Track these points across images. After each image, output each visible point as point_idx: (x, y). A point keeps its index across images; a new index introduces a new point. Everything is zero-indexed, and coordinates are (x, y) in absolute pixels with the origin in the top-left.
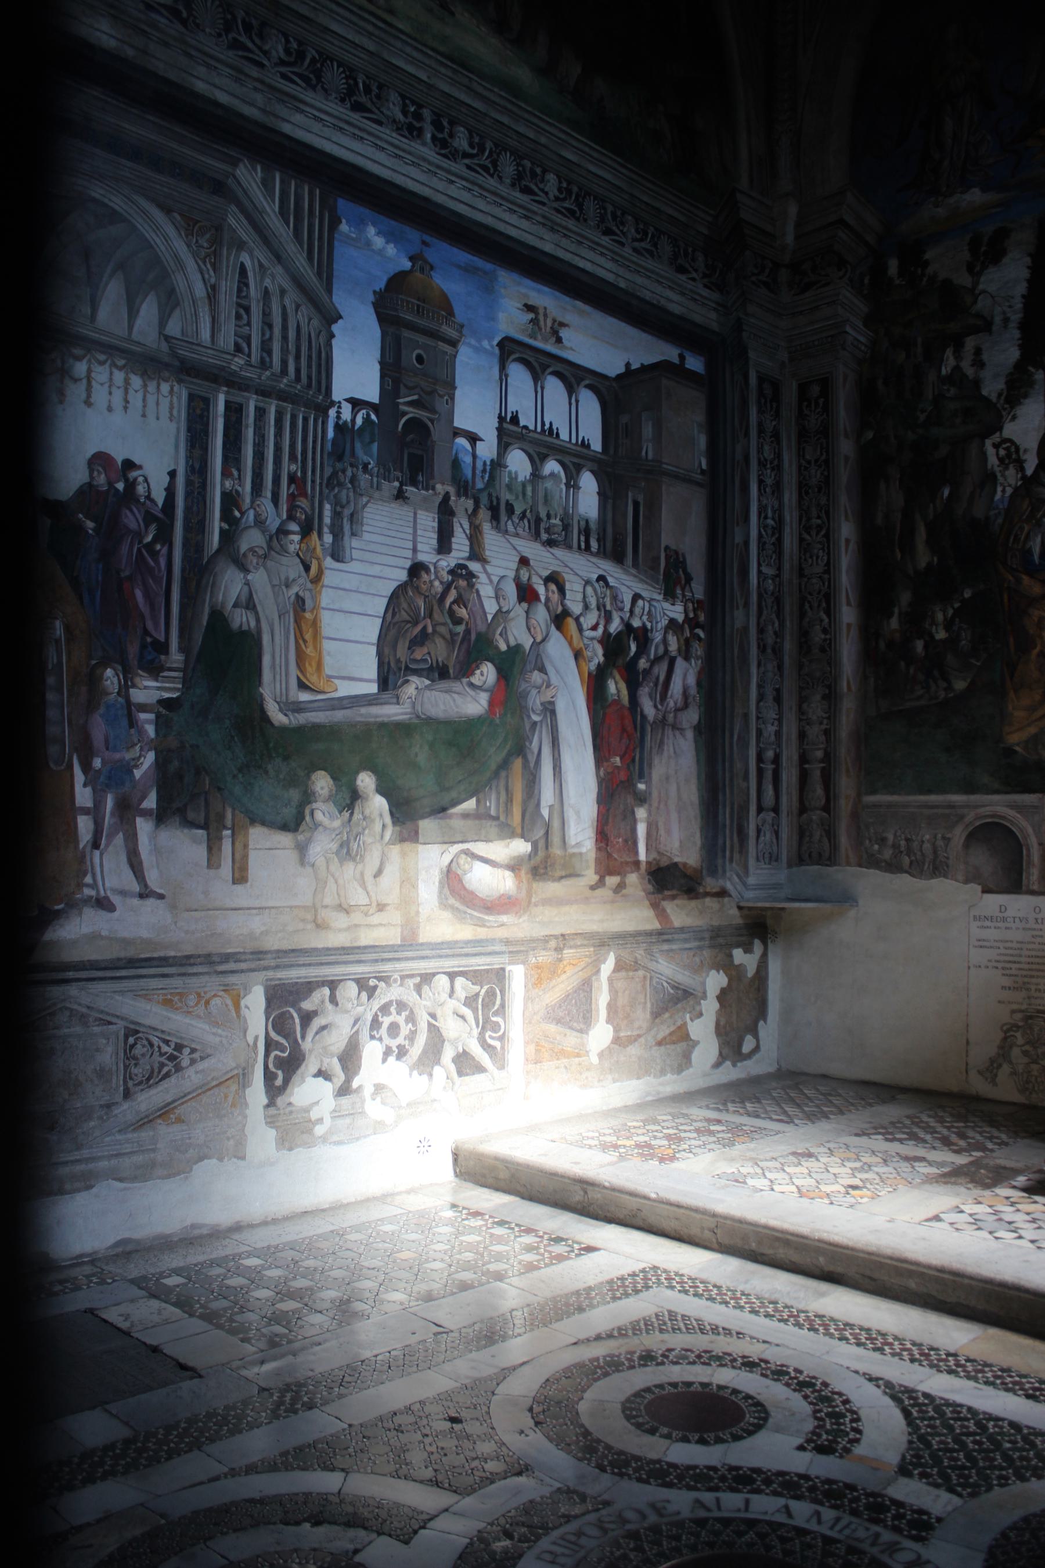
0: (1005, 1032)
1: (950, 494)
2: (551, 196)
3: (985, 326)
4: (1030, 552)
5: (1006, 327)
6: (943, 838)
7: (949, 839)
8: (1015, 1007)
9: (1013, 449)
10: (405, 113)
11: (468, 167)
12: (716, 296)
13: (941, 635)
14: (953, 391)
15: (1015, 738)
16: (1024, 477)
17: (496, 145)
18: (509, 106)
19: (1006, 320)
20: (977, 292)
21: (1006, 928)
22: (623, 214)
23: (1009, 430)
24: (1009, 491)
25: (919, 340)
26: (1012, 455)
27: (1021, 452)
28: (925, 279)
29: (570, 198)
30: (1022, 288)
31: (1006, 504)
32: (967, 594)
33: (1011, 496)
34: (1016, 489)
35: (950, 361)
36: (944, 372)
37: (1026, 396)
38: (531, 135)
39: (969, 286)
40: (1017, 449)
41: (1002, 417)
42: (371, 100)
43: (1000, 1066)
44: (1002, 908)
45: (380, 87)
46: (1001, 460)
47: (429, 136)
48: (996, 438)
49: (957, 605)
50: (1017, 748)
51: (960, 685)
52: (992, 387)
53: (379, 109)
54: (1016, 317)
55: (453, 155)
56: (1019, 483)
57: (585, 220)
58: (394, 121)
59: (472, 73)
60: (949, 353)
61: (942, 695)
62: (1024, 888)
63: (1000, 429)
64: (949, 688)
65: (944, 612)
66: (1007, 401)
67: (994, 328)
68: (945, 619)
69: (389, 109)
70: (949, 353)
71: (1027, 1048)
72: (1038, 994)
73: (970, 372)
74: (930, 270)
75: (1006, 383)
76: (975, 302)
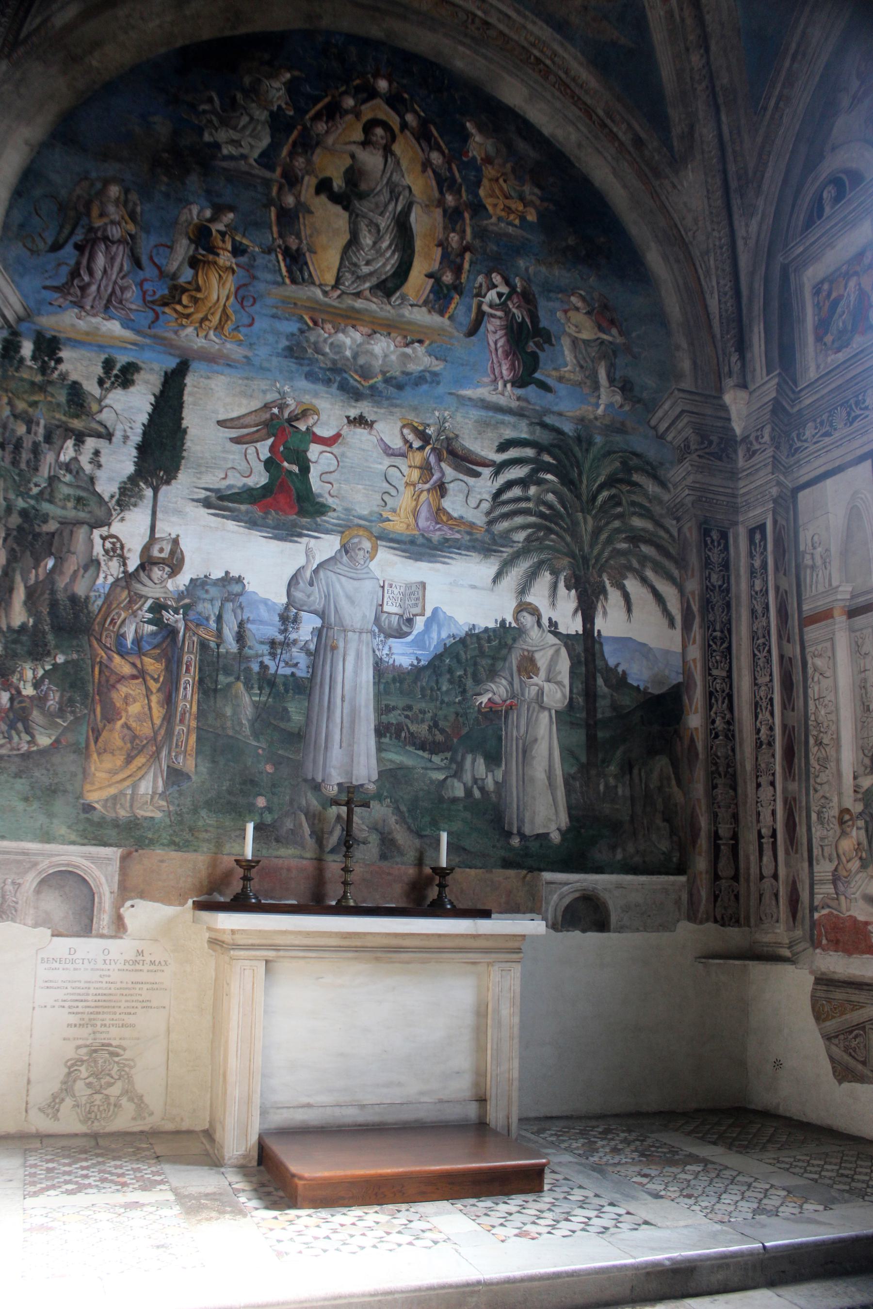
0: (69, 1068)
1: (54, 566)
3: (109, 436)
4: (123, 636)
5: (124, 442)
6: (13, 883)
7: (19, 884)
8: (80, 1042)
9: (118, 545)
13: (28, 691)
14: (68, 478)
15: (95, 796)
16: (125, 572)
19: (126, 438)
20: (103, 404)
21: (75, 969)
23: (116, 528)
24: (111, 580)
25: (42, 422)
26: (117, 550)
27: (125, 551)
28: (56, 373)
30: (144, 418)
31: (107, 590)
32: (60, 659)
33: (113, 584)
34: (117, 580)
35: (68, 452)
36: (62, 458)
37: (135, 505)
39: (98, 396)
40: (122, 547)
41: (111, 515)
43: (63, 1100)
44: (72, 951)
46: (107, 552)
48: (104, 531)
49: (48, 667)
50: (96, 805)
51: (44, 741)
52: (107, 487)
54: (136, 438)
56: (121, 575)
60: (70, 443)
61: (25, 747)
62: (94, 932)
63: (109, 525)
64: (33, 742)
65: (34, 670)
66: (119, 503)
67: (114, 439)
68: (35, 678)
70: (70, 443)
71: (91, 1079)
72: (103, 1029)
73: (88, 468)
74: (62, 367)
75: (120, 488)
76: (101, 411)
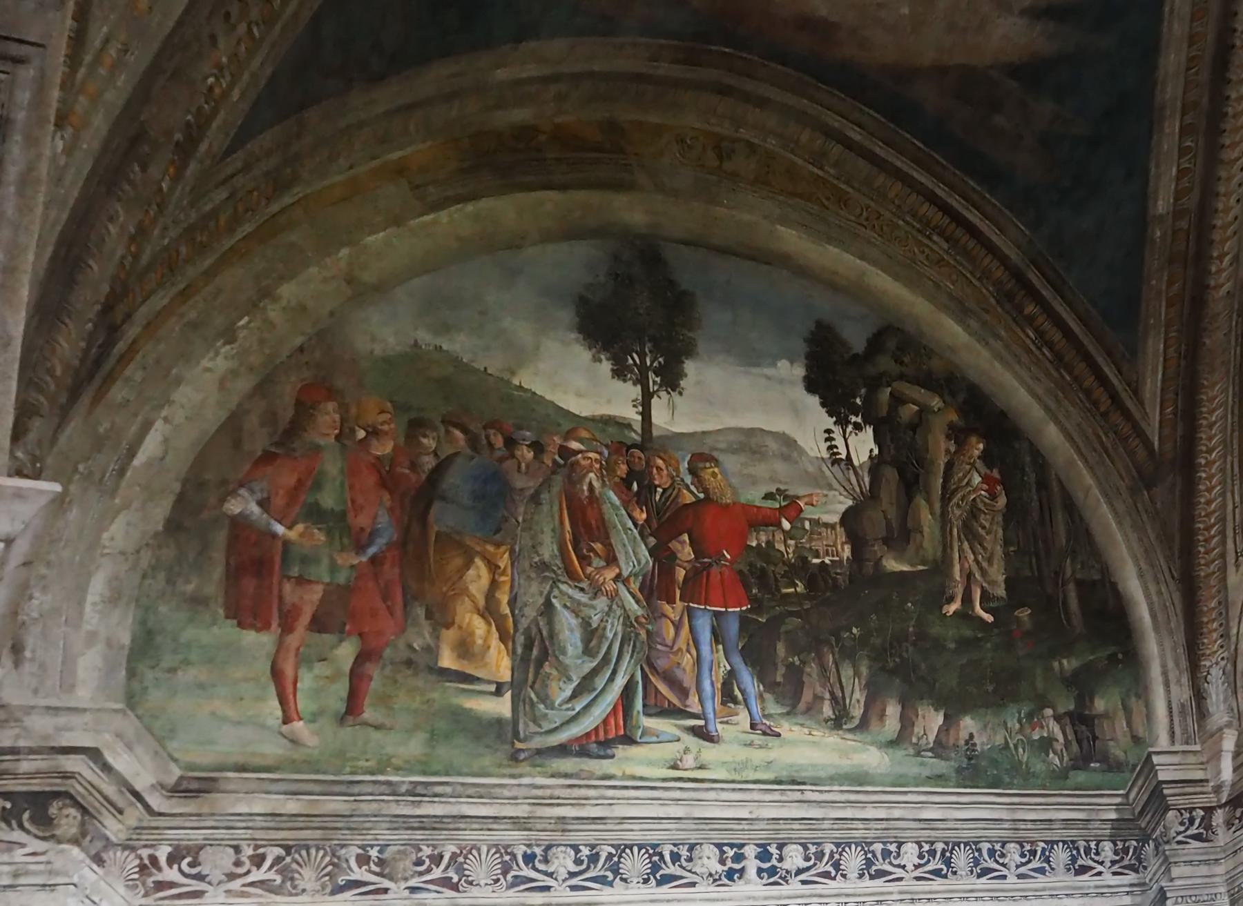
2: (910, 867)
10: (722, 862)
11: (804, 882)
12: (1131, 877)
17: (837, 845)
18: (853, 797)
22: (1004, 844)
29: (934, 859)
38: (882, 814)
42: (681, 866)
45: (692, 848)
47: (752, 872)
53: (690, 871)
55: (784, 879)
57: (955, 873)
58: (711, 875)
59: (804, 784)
69: (703, 865)
